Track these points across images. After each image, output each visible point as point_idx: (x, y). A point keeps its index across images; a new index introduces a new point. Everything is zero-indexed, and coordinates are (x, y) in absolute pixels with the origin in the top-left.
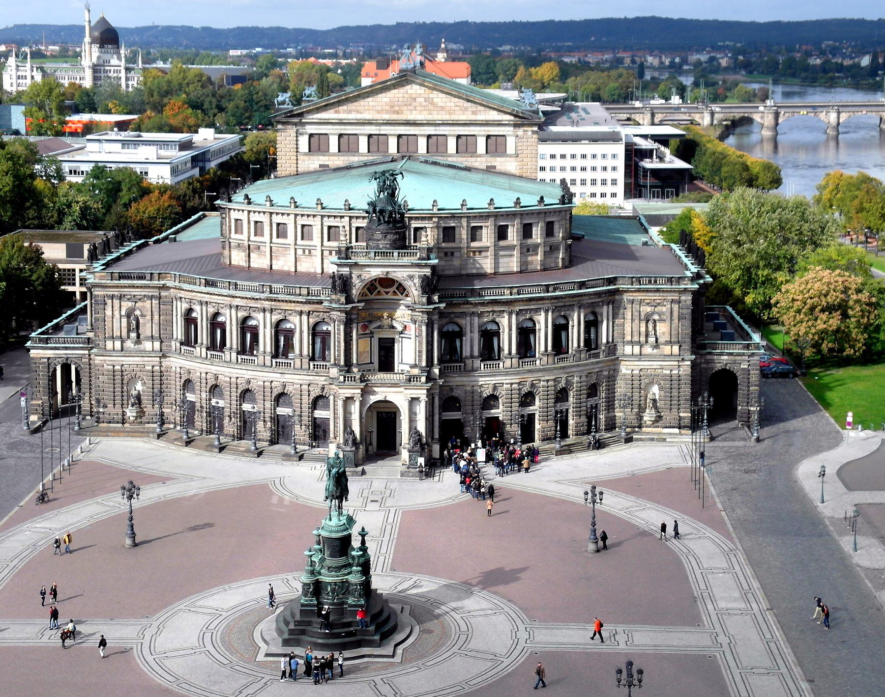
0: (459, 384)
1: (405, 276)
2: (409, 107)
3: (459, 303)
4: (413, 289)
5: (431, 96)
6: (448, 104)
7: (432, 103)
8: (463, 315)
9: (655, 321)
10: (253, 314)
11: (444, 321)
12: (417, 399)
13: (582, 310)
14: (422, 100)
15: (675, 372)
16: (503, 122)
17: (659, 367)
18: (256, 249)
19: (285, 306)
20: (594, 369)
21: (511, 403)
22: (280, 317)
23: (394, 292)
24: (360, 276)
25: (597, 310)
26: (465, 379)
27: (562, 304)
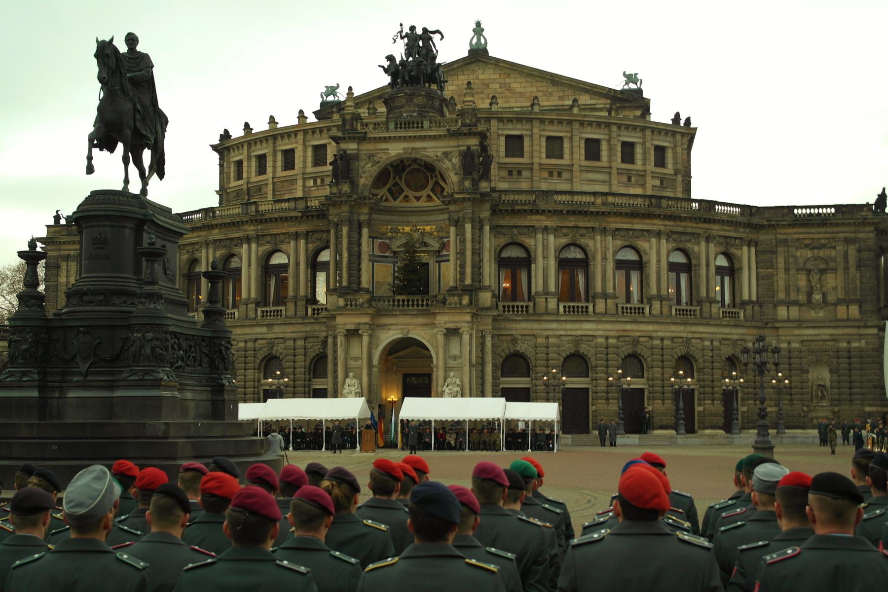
0: (526, 332)
1: (439, 154)
2: (481, 96)
3: (525, 211)
4: (452, 174)
6: (529, 90)
7: (509, 89)
8: (532, 230)
10: (236, 250)
13: (711, 245)
14: (497, 86)
15: (855, 345)
16: (597, 106)
17: (829, 338)
18: (256, 192)
20: (731, 334)
22: (266, 248)
23: (429, 196)
25: (733, 250)
26: (535, 325)
27: (680, 229)
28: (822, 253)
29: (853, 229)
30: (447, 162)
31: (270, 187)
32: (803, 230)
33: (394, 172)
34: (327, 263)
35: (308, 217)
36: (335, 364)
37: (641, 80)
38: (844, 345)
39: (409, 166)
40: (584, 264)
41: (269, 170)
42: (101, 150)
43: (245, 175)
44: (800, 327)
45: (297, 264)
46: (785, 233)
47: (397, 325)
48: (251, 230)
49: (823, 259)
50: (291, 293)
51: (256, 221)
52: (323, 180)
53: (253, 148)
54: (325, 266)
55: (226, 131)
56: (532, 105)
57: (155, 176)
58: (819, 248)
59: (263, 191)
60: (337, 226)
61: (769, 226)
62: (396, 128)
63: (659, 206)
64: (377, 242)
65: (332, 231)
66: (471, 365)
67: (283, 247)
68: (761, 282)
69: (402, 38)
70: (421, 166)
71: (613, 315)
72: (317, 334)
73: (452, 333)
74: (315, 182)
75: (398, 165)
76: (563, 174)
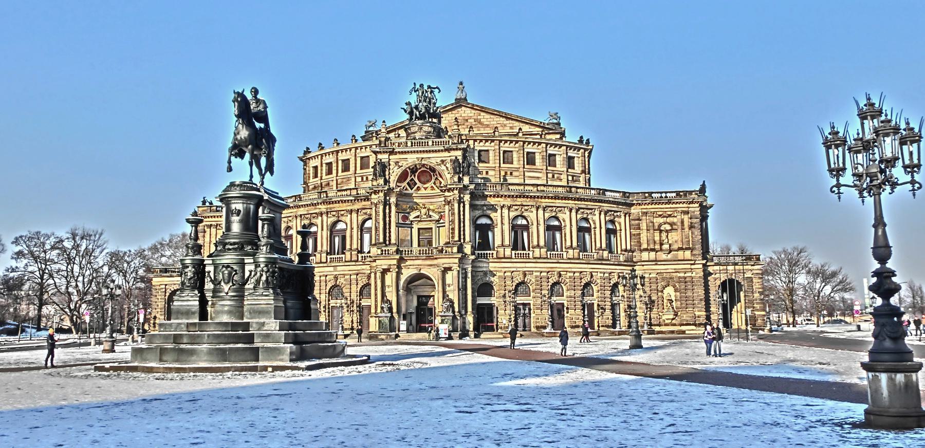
1: (438, 161)
2: (463, 126)
5: (479, 117)
6: (492, 123)
7: (480, 122)
9: (667, 231)
10: (313, 221)
11: (478, 213)
12: (450, 269)
14: (473, 120)
15: (689, 274)
17: (674, 271)
19: (337, 207)
21: (541, 290)
22: (335, 219)
23: (432, 187)
24: (398, 162)
28: (669, 220)
29: (687, 205)
30: (442, 166)
31: (335, 182)
32: (657, 206)
33: (411, 172)
34: (371, 228)
35: (358, 200)
36: (376, 290)
37: (560, 117)
38: (682, 275)
39: (420, 168)
40: (526, 228)
41: (334, 172)
42: (236, 157)
43: (319, 175)
44: (656, 264)
45: (352, 229)
46: (646, 209)
47: (413, 265)
48: (323, 208)
49: (669, 224)
50: (348, 247)
51: (327, 203)
52: (367, 178)
53: (324, 157)
54: (369, 230)
55: (308, 148)
56: (494, 132)
57: (268, 173)
58: (667, 217)
59: (331, 183)
60: (376, 205)
61: (637, 204)
62: (412, 146)
63: (571, 192)
64: (401, 215)
65: (374, 209)
66: (459, 289)
67: (343, 218)
68: (633, 237)
69: (415, 91)
70: (427, 168)
71: (544, 258)
72: (364, 271)
73: (447, 270)
74: (362, 179)
75: (413, 168)
76: (513, 173)
